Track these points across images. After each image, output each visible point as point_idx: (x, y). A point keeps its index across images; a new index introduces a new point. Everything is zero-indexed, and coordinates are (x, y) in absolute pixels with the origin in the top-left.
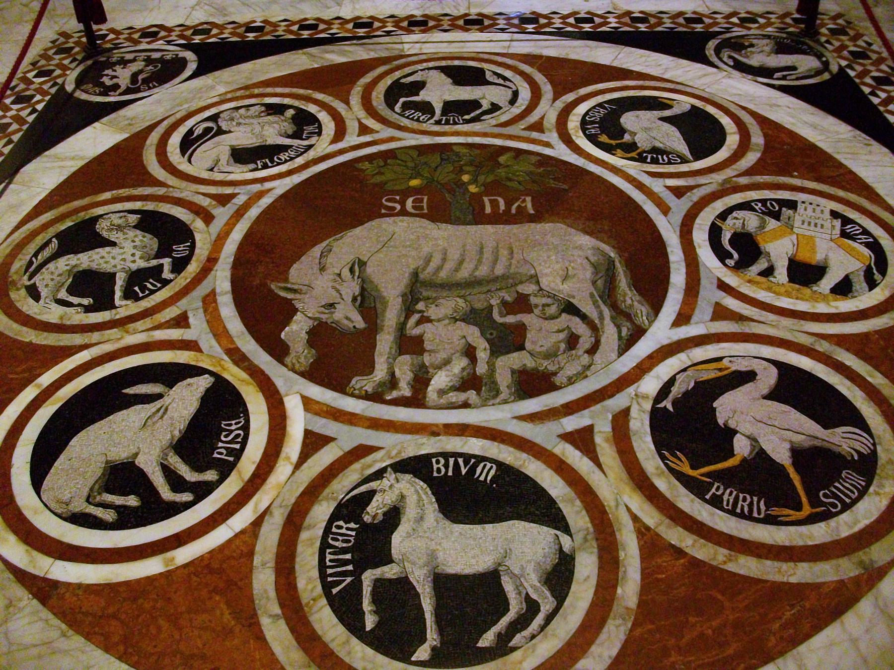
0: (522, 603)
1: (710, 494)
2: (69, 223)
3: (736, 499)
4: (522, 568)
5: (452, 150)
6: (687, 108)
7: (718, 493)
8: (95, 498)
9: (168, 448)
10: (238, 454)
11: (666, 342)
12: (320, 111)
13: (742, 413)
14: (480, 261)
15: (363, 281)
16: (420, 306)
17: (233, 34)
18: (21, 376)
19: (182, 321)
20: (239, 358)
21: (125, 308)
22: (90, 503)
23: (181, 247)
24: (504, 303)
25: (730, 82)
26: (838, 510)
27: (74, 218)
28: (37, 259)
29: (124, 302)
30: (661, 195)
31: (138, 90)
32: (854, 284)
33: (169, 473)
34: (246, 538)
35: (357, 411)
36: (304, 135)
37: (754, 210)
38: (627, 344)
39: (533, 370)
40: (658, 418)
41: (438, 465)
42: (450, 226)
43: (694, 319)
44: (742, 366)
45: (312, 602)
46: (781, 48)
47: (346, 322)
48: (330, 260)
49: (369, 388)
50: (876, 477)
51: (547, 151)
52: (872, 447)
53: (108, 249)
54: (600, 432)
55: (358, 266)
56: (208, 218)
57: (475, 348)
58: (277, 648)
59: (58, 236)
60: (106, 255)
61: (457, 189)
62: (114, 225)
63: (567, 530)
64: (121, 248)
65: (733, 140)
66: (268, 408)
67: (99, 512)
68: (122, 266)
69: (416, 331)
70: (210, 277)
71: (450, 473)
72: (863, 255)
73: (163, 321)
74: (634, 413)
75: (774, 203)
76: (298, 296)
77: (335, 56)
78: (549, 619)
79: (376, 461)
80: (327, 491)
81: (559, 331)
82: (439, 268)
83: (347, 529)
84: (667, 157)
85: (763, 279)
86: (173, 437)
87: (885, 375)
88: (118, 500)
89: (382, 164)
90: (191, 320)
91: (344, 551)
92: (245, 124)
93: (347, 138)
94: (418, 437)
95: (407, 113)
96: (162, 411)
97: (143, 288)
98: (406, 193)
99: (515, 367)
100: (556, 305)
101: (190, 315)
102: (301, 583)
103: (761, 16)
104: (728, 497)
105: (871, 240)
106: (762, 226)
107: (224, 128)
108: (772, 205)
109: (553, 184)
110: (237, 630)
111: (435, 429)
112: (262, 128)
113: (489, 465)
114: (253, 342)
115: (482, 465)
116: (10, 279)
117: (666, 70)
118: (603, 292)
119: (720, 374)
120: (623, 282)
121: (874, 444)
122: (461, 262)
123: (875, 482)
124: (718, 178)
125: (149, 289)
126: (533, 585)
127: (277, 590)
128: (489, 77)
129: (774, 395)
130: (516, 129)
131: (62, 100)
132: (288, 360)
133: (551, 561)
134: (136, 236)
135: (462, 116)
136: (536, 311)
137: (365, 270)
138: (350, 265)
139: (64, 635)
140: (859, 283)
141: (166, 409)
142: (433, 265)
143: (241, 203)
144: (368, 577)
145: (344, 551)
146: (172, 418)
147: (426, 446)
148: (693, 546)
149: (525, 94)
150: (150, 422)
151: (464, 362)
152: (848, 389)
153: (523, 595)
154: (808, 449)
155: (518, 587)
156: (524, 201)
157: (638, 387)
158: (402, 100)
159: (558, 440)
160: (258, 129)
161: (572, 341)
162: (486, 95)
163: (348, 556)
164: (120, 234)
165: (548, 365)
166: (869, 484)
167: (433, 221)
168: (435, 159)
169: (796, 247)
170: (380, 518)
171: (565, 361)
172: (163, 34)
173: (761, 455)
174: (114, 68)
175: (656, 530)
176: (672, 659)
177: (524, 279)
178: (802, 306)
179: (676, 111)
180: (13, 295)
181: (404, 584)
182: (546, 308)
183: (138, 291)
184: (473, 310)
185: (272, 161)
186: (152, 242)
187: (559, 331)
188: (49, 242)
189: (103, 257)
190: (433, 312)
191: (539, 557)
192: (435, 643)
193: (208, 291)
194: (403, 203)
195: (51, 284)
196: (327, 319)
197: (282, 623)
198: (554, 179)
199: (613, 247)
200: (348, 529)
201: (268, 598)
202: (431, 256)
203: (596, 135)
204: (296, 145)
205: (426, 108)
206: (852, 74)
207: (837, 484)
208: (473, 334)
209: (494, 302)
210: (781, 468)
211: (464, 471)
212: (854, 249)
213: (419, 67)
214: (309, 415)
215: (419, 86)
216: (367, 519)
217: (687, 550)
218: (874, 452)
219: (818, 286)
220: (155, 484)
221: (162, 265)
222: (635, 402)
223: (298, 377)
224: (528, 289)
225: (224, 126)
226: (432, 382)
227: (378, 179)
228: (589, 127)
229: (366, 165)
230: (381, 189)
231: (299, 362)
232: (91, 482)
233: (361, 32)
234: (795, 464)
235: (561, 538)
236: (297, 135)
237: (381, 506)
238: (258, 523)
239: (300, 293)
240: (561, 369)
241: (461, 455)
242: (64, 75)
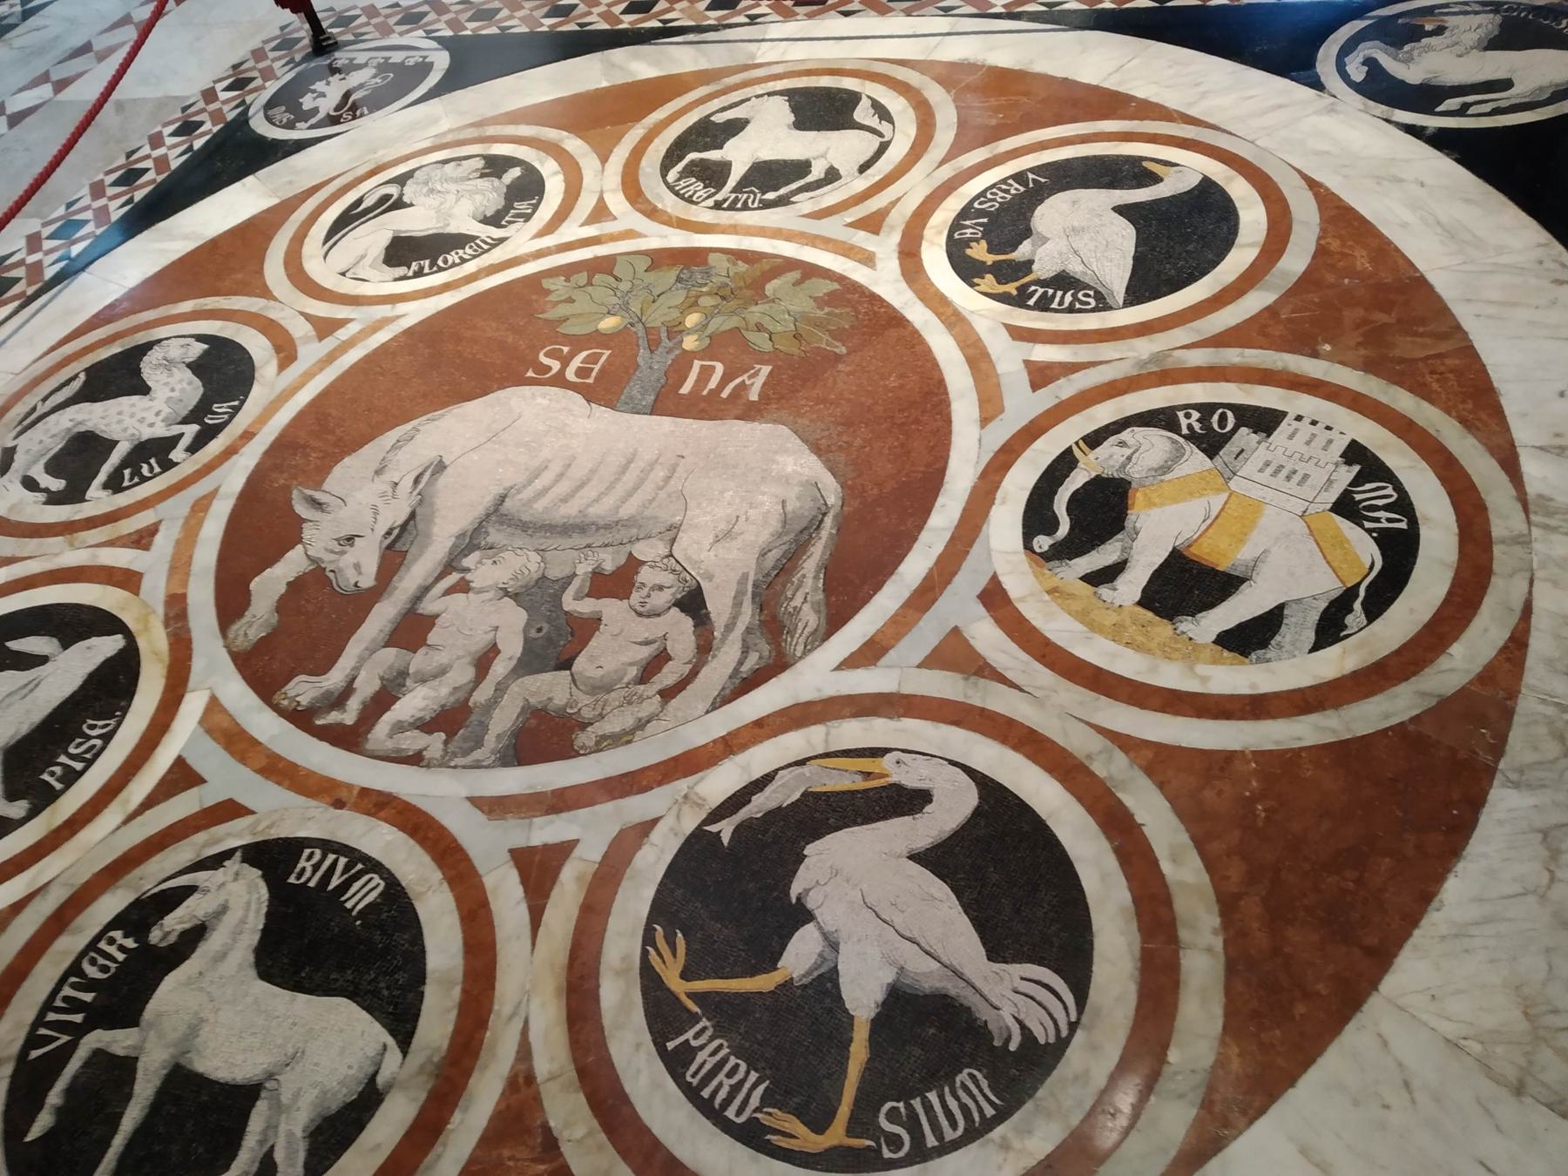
1: (681, 1039)
2: (116, 349)
3: (724, 1061)
5: (705, 263)
6: (1192, 181)
7: (694, 1043)
10: (71, 777)
13: (848, 881)
14: (611, 487)
15: (421, 502)
16: (468, 562)
24: (597, 575)
25: (1327, 123)
26: (901, 1154)
32: (1283, 628)
36: (507, 219)
37: (1172, 426)
48: (402, 455)
49: (304, 701)
50: (1029, 1106)
52: (1064, 1033)
57: (498, 652)
61: (666, 343)
62: (166, 359)
63: (404, 1040)
75: (1230, 414)
79: (235, 835)
80: (137, 872)
81: (647, 643)
82: (545, 490)
85: (1086, 588)
87: (1210, 865)
91: (89, 985)
94: (312, 803)
95: (682, 183)
96: (31, 686)
97: (137, 472)
98: (578, 343)
99: (533, 701)
100: (673, 590)
101: (162, 528)
105: (1403, 525)
106: (1165, 469)
107: (406, 199)
108: (1223, 418)
109: (824, 341)
111: (343, 794)
118: (768, 575)
119: (860, 784)
121: (1073, 1027)
123: (1017, 1116)
124: (1145, 347)
128: (862, 114)
129: (934, 859)
133: (345, 1095)
134: (181, 381)
135: (763, 194)
136: (636, 597)
137: (436, 480)
140: (1299, 629)
141: (37, 685)
142: (538, 484)
143: (344, 338)
145: (89, 985)
148: (580, 1141)
151: (469, 674)
153: (265, 1149)
154: (926, 996)
155: (271, 1127)
159: (507, 857)
160: (451, 198)
163: (88, 997)
165: (585, 705)
166: (1002, 1116)
167: (589, 401)
169: (1209, 522)
170: (172, 939)
171: (617, 703)
173: (826, 984)
175: (542, 1089)
177: (655, 531)
181: (120, 1070)
187: (647, 643)
188: (76, 377)
191: (333, 1084)
193: (211, 488)
194: (565, 362)
196: (331, 562)
200: (122, 948)
202: (546, 467)
203: (967, 243)
204: (483, 236)
207: (932, 1096)
211: (335, 882)
212: (1341, 541)
213: (759, 90)
215: (736, 127)
217: (566, 1149)
218: (1062, 1045)
222: (675, 808)
224: (647, 551)
225: (409, 193)
226: (397, 706)
228: (968, 223)
230: (551, 333)
231: (246, 634)
234: (879, 1024)
235: (387, 1055)
236: (495, 220)
240: (602, 716)
242: (262, 88)
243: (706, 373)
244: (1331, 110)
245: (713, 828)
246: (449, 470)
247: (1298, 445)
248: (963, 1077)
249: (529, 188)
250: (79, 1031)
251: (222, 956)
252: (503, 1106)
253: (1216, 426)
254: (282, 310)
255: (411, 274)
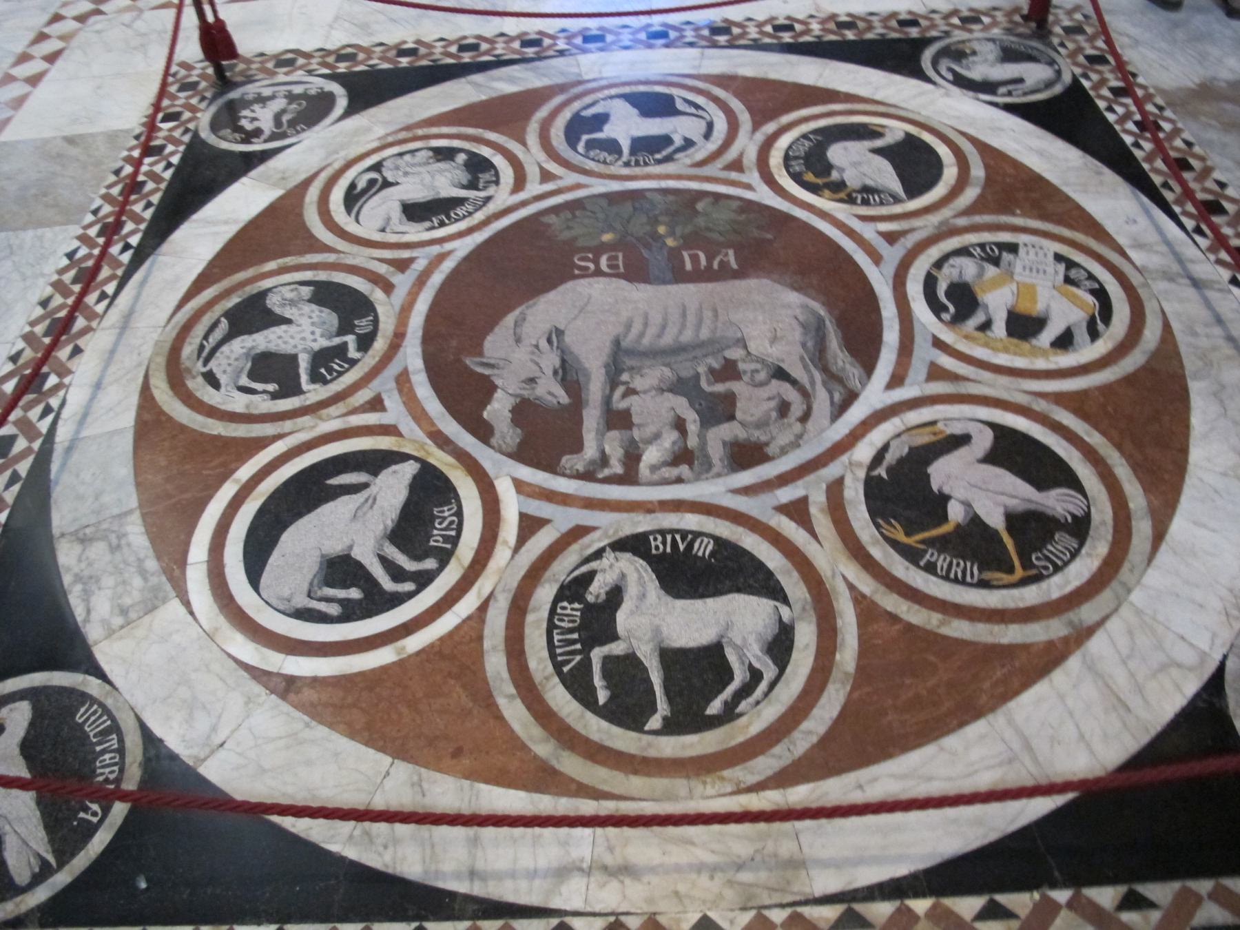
0: (745, 672)
2: (235, 300)
3: (950, 565)
4: (744, 639)
5: (645, 197)
6: (899, 136)
7: (933, 559)
8: (316, 593)
9: (382, 538)
10: (455, 541)
11: (879, 406)
12: (494, 155)
14: (683, 326)
15: (563, 352)
16: (625, 377)
17: (382, 59)
18: (218, 470)
19: (376, 404)
20: (442, 440)
21: (314, 393)
22: (312, 598)
23: (364, 322)
24: (712, 371)
25: (948, 101)
27: (240, 293)
28: (208, 342)
29: (312, 387)
30: (873, 243)
31: (284, 136)
33: (385, 561)
34: (473, 624)
35: (570, 491)
37: (970, 255)
38: (841, 409)
39: (745, 440)
40: (872, 487)
41: (656, 543)
42: (648, 287)
43: (908, 381)
44: (957, 429)
45: (544, 681)
46: (1009, 55)
47: (549, 398)
48: (526, 329)
49: (580, 467)
51: (748, 195)
52: (1086, 509)
53: (284, 327)
54: (815, 502)
55: (556, 335)
56: (388, 288)
57: (684, 420)
58: (516, 727)
59: (228, 314)
60: (283, 335)
61: (654, 244)
62: (286, 300)
63: (785, 601)
64: (298, 325)
65: (950, 173)
66: (480, 493)
67: (322, 607)
68: (303, 346)
69: (622, 405)
70: (400, 354)
71: (668, 550)
72: (1088, 304)
73: (357, 405)
74: (848, 481)
75: (994, 247)
76: (496, 371)
77: (503, 83)
78: (772, 685)
80: (548, 574)
81: (769, 399)
82: (642, 335)
83: (572, 610)
84: (880, 197)
86: (385, 528)
87: (1104, 433)
88: (341, 594)
89: (569, 216)
90: (387, 403)
91: (571, 631)
92: (413, 174)
93: (529, 186)
94: (633, 515)
95: (592, 154)
96: (370, 501)
97: (330, 371)
98: (599, 250)
99: (727, 439)
101: (385, 396)
102: (533, 664)
103: (986, 14)
104: (942, 562)
105: (1097, 286)
106: (981, 274)
107: (390, 179)
108: (992, 250)
109: (756, 233)
110: (475, 712)
111: (650, 506)
112: (433, 177)
113: (706, 540)
114: (454, 423)
115: (699, 541)
116: (183, 366)
117: (877, 89)
119: (933, 438)
120: (834, 342)
121: (1089, 507)
122: (664, 327)
124: (934, 219)
125: (337, 371)
126: (756, 655)
127: (510, 671)
128: (680, 105)
129: (991, 458)
130: (713, 170)
131: (197, 152)
132: (494, 441)
136: (746, 378)
138: (546, 335)
139: (307, 725)
140: (1081, 335)
141: (375, 499)
144: (597, 654)
145: (571, 631)
146: (382, 508)
147: (641, 524)
148: (908, 611)
149: (721, 126)
150: (360, 513)
151: (675, 435)
152: (1065, 449)
155: (742, 658)
156: (726, 255)
157: (851, 455)
158: (585, 137)
159: (774, 512)
160: (428, 178)
161: (784, 408)
162: (679, 128)
163: (575, 636)
164: (294, 310)
165: (759, 436)
166: (1081, 544)
168: (627, 208)
170: (603, 597)
172: (301, 61)
173: (976, 521)
174: (252, 108)
176: (890, 718)
178: (1020, 363)
179: (888, 140)
180: (190, 384)
181: (631, 660)
182: (755, 375)
183: (325, 373)
184: (680, 379)
185: (449, 217)
186: (331, 318)
187: (769, 399)
189: (280, 337)
190: (638, 383)
191: (760, 628)
192: (665, 713)
194: (597, 263)
195: (229, 369)
197: (518, 704)
198: (758, 228)
199: (823, 304)
200: (572, 609)
201: (502, 680)
204: (473, 197)
205: (612, 147)
206: (1086, 84)
207: (1050, 547)
208: (681, 405)
209: (702, 369)
210: (996, 532)
211: (682, 547)
213: (600, 95)
214: (522, 498)
215: (601, 120)
216: (590, 598)
218: (1088, 515)
219: (1038, 340)
220: (375, 576)
221: (345, 344)
222: (849, 470)
223: (505, 458)
224: (735, 354)
226: (644, 458)
227: (566, 235)
229: (552, 219)
230: (570, 248)
231: (505, 443)
232: (310, 577)
233: (530, 51)
236: (472, 185)
237: (603, 585)
238: (483, 607)
239: (498, 369)
240: (773, 438)
241: (677, 531)
243: (695, 259)
244: (947, 95)
245: (875, 473)
246: (567, 332)
247: (1032, 256)
248: (1057, 537)
249: (478, 167)
250: (586, 650)
251: (643, 596)
252: (858, 610)
253: (991, 253)
254: (354, 258)
255: (436, 225)
